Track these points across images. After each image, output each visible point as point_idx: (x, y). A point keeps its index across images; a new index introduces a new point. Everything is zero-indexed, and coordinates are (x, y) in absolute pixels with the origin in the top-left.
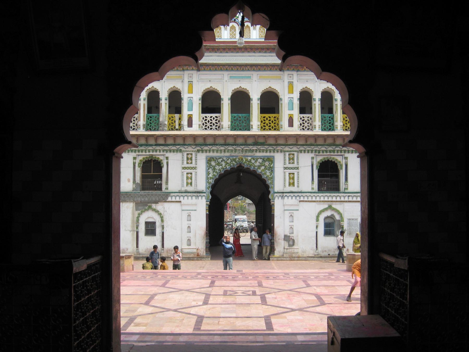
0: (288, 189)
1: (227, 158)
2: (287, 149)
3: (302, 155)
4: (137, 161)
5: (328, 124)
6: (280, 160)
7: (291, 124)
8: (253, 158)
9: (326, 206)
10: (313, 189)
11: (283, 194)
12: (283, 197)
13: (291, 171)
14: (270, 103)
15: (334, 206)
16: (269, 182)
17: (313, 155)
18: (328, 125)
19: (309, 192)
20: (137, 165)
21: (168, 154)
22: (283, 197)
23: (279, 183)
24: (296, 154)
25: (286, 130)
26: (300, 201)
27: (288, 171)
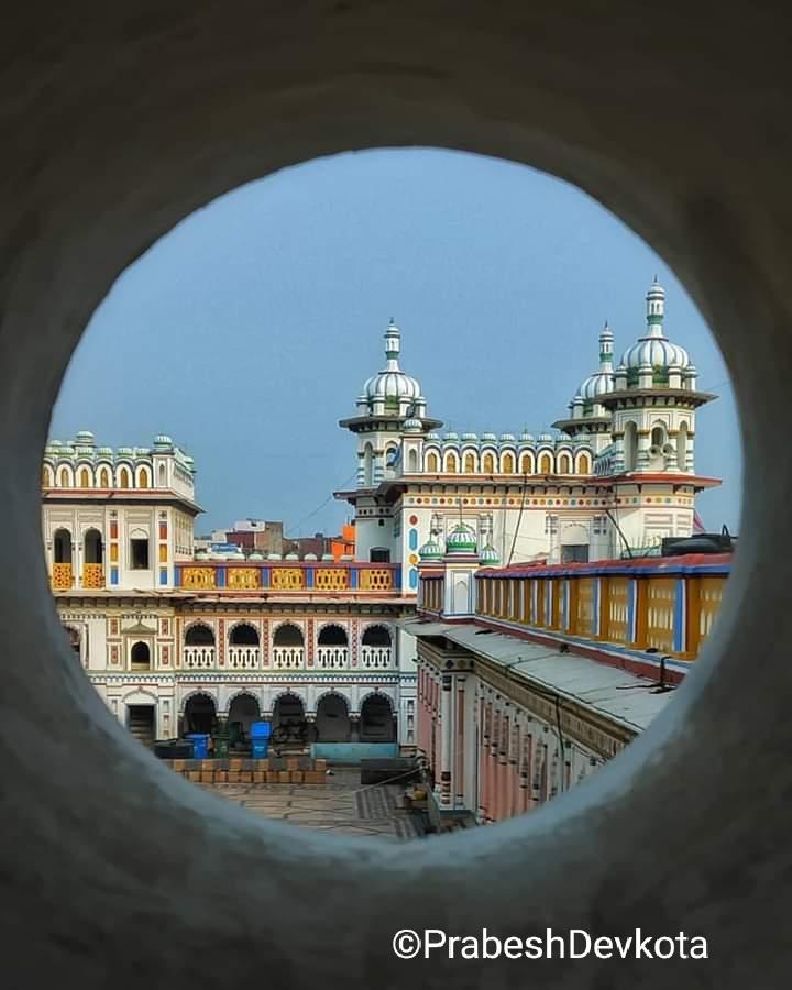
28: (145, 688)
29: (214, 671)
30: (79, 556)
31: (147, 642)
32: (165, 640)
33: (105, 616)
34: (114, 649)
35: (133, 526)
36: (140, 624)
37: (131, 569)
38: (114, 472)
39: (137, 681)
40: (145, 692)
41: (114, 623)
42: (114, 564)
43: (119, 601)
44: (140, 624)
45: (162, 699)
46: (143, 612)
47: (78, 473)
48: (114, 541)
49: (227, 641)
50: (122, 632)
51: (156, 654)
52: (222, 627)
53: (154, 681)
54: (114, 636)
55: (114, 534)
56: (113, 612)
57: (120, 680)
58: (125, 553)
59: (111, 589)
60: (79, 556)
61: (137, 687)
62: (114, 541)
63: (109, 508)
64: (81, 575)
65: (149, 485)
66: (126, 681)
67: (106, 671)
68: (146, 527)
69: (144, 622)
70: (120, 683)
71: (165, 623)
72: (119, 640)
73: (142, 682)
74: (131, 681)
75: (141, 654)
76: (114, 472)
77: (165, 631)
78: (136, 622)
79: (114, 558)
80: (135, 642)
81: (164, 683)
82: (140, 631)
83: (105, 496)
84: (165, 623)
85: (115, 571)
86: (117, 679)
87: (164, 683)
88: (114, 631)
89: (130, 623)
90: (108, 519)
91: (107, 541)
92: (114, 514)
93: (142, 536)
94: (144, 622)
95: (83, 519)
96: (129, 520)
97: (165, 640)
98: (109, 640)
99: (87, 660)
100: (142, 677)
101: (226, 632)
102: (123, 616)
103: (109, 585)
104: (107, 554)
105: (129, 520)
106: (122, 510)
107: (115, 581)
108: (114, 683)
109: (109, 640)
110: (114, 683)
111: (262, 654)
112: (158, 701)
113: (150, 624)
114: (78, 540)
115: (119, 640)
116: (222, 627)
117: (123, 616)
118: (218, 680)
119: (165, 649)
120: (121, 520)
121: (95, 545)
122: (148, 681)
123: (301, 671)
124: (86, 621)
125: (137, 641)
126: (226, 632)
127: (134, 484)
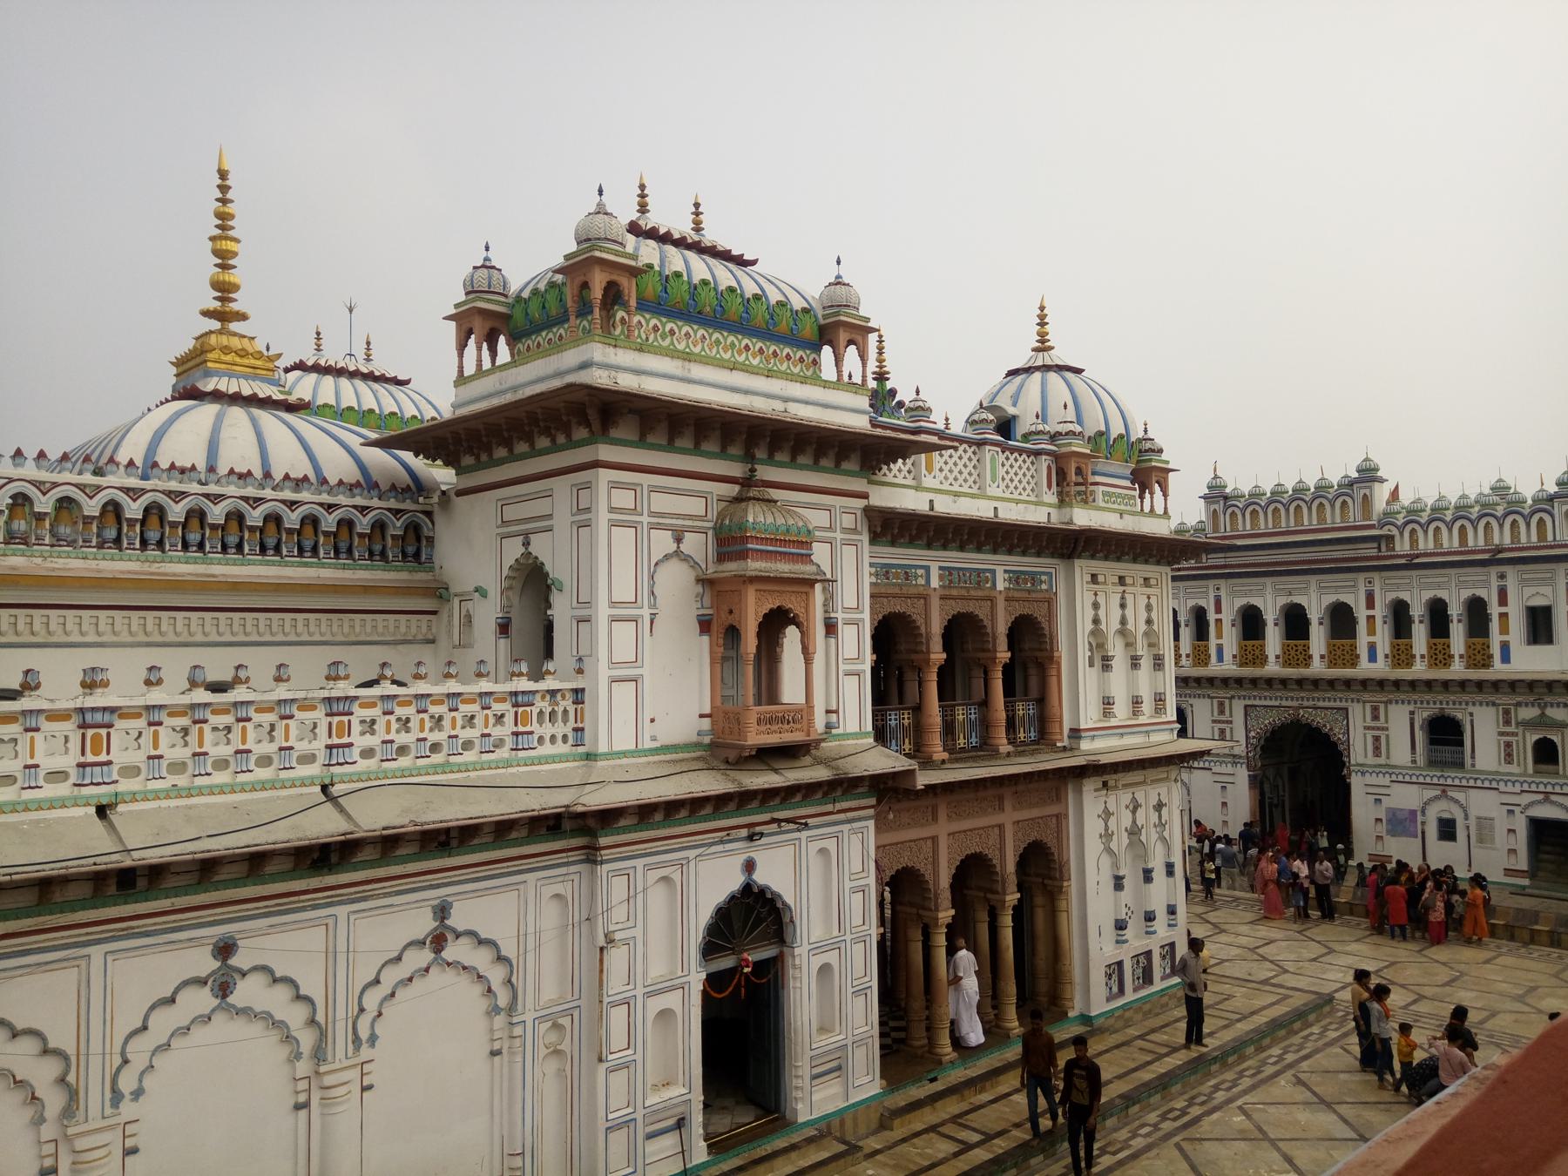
0: (1371, 760)
1: (1277, 708)
2: (1366, 696)
3: (1392, 708)
5: (1440, 657)
6: (1358, 715)
7: (1372, 658)
8: (1316, 711)
10: (1414, 762)
11: (1364, 770)
12: (1363, 774)
13: (1377, 733)
14: (1341, 620)
16: (1341, 747)
17: (1411, 708)
18: (1440, 657)
21: (1191, 701)
22: (1363, 774)
23: (1359, 750)
25: (1366, 668)
27: (1370, 734)
28: (1553, 798)
30: (1458, 633)
31: (1554, 738)
33: (1494, 704)
34: (1508, 745)
35: (1528, 591)
37: (1529, 643)
38: (1528, 525)
39: (1542, 788)
41: (1507, 712)
42: (1505, 638)
43: (1513, 685)
46: (1548, 699)
47: (1406, 535)
48: (1503, 610)
50: (1518, 724)
54: (1508, 729)
55: (1503, 601)
56: (1505, 700)
59: (1499, 670)
60: (1458, 633)
61: (1541, 797)
62: (1503, 610)
63: (1494, 571)
64: (1424, 651)
65: (1550, 538)
66: (1526, 787)
67: (1497, 773)
68: (1547, 590)
69: (1550, 712)
70: (1518, 788)
72: (1513, 734)
74: (1534, 787)
76: (1528, 525)
79: (1504, 630)
80: (1536, 737)
82: (1542, 722)
83: (1486, 556)
85: (1505, 647)
88: (1507, 722)
90: (1495, 584)
91: (1494, 610)
92: (1502, 576)
93: (1538, 602)
94: (1550, 712)
95: (1462, 585)
96: (1524, 583)
98: (1502, 734)
99: (1473, 757)
100: (1546, 782)
104: (1495, 626)
105: (1524, 583)
106: (1510, 571)
107: (1506, 658)
109: (1502, 734)
110: (1510, 788)
114: (1455, 610)
115: (1513, 734)
117: (1518, 704)
120: (1512, 584)
121: (1477, 612)
122: (1557, 789)
124: (1471, 709)
127: (1529, 536)
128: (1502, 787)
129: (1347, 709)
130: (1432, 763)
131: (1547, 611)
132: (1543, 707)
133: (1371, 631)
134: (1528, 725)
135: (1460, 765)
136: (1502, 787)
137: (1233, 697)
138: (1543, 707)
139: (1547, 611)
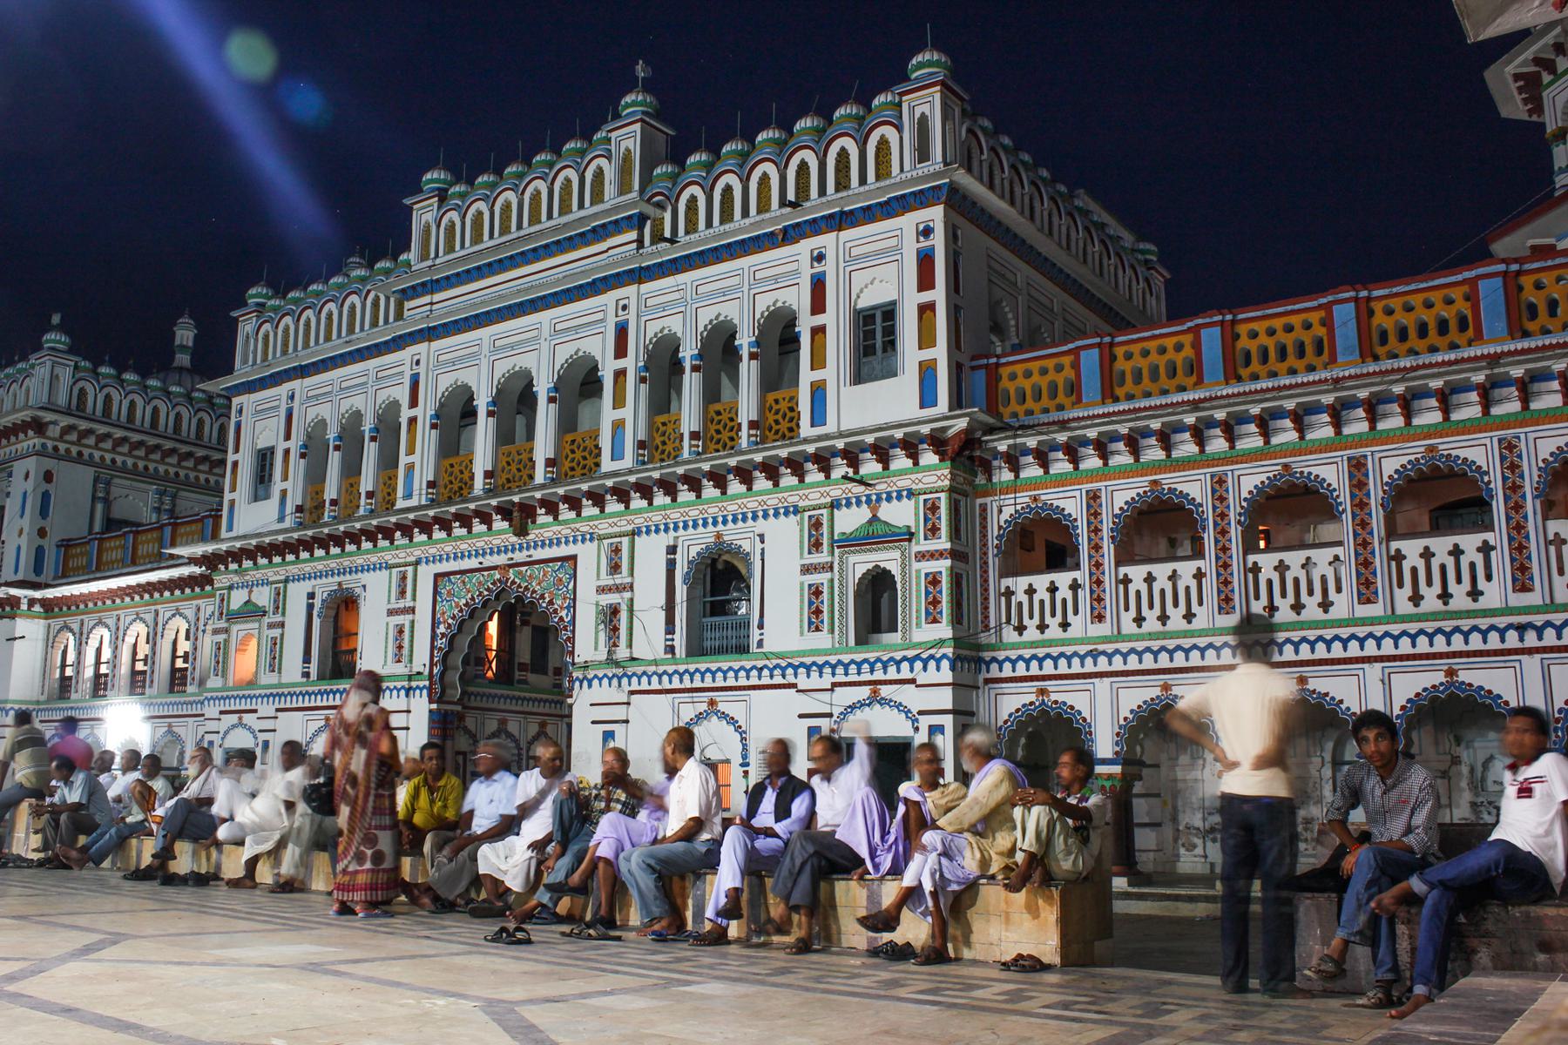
4: (317, 602)
7: (617, 455)
9: (704, 707)
15: (721, 707)
19: (655, 662)
20: (315, 613)
24: (625, 540)
26: (632, 693)
28: (885, 691)
29: (1082, 641)
32: (933, 555)
36: (875, 518)
40: (884, 702)
41: (816, 524)
44: (875, 518)
45: (925, 722)
49: (1108, 549)
51: (911, 599)
52: (1094, 514)
53: (905, 673)
57: (827, 670)
58: (839, 345)
61: (864, 692)
70: (827, 680)
71: (933, 508)
73: (879, 675)
75: (876, 604)
77: (933, 531)
78: (864, 514)
79: (818, 362)
81: (932, 675)
84: (933, 508)
85: (818, 390)
86: (821, 668)
87: (932, 675)
88: (816, 545)
89: (850, 520)
97: (933, 555)
98: (806, 570)
101: (1106, 526)
102: (834, 505)
103: (806, 430)
107: (818, 418)
108: (815, 681)
111: (1211, 584)
112: (917, 729)
113: (900, 514)
116: (1094, 514)
117: (834, 505)
118: (1089, 667)
119: (934, 580)
123: (1340, 623)
125: (870, 566)
126: (1106, 526)
128: (802, 681)
129: (574, 558)
130: (697, 649)
131: (889, 312)
132: (873, 503)
133: (619, 402)
134: (852, 542)
135: (743, 649)
136: (802, 681)
137: (417, 563)
138: (873, 503)
139: (889, 312)
